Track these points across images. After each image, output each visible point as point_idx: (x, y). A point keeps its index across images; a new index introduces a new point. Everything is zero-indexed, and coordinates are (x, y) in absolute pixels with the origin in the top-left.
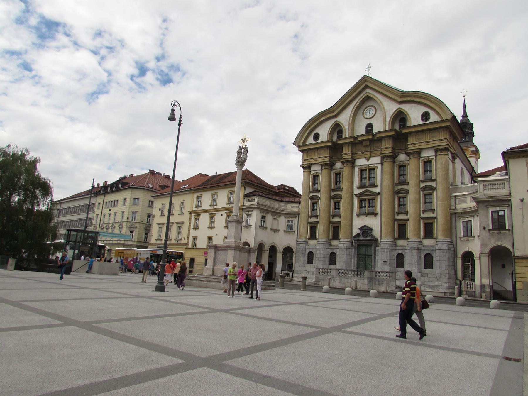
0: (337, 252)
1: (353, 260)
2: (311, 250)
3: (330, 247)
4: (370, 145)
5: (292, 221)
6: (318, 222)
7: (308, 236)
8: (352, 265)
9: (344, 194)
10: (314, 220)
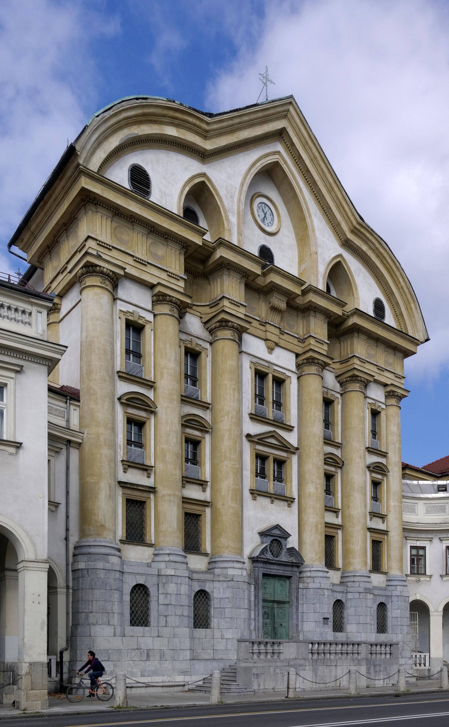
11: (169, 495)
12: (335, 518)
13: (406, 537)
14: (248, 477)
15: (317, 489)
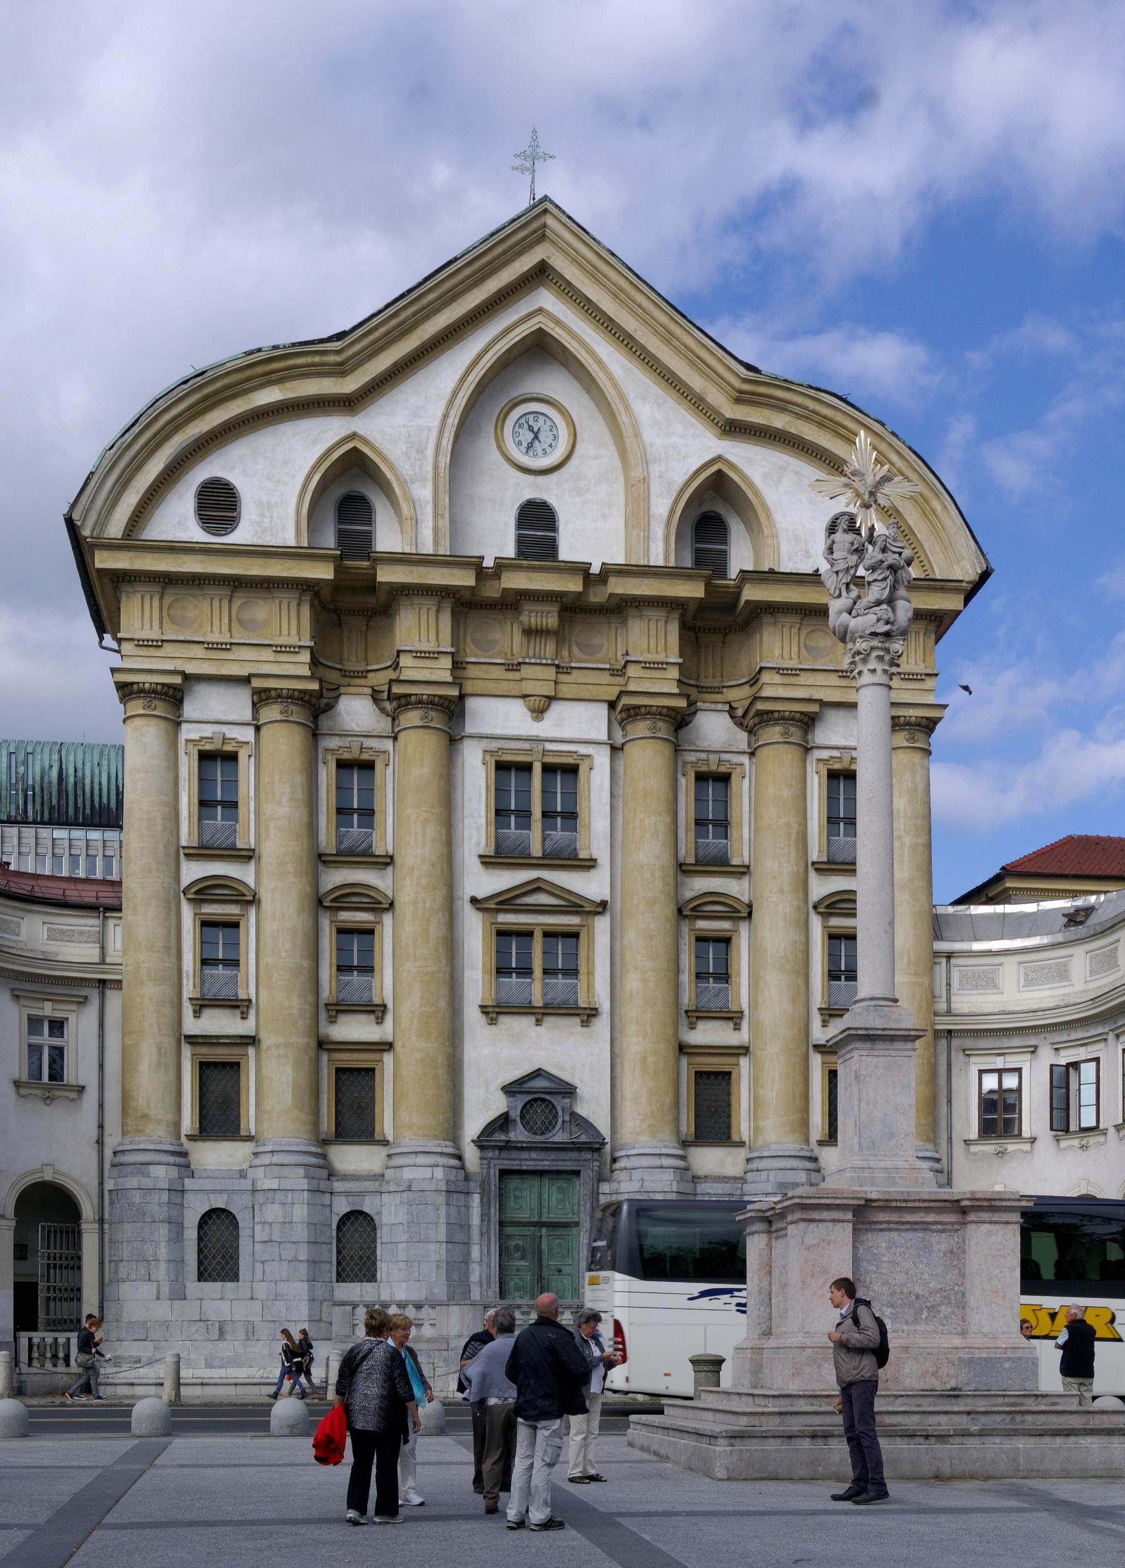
0: (390, 1214)
1: (475, 1253)
2: (220, 1204)
3: (338, 1186)
4: (559, 635)
5: (57, 1026)
6: (252, 1040)
7: (189, 1121)
8: (474, 1277)
9: (409, 885)
10: (220, 1023)
11: (277, 1046)
12: (731, 1032)
13: (964, 1050)
14: (477, 981)
15: (645, 981)
